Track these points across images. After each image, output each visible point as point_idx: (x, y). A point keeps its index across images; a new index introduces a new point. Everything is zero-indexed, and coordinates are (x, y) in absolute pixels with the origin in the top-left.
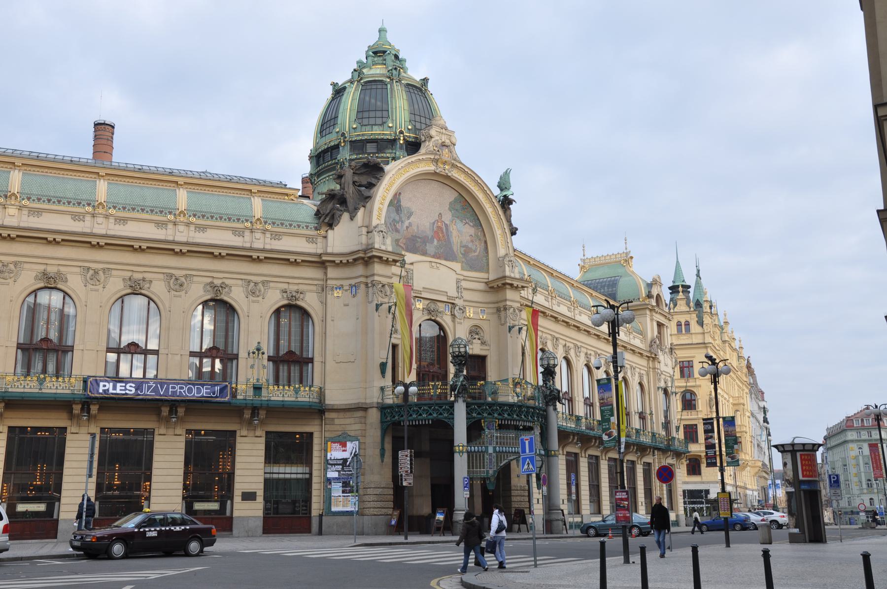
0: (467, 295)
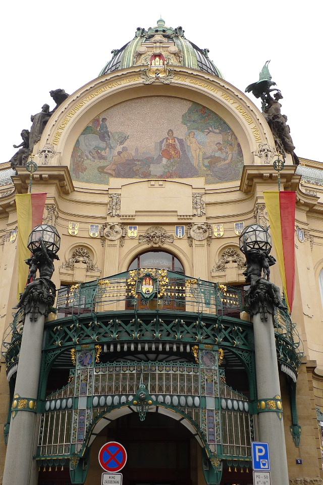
0: (213, 212)
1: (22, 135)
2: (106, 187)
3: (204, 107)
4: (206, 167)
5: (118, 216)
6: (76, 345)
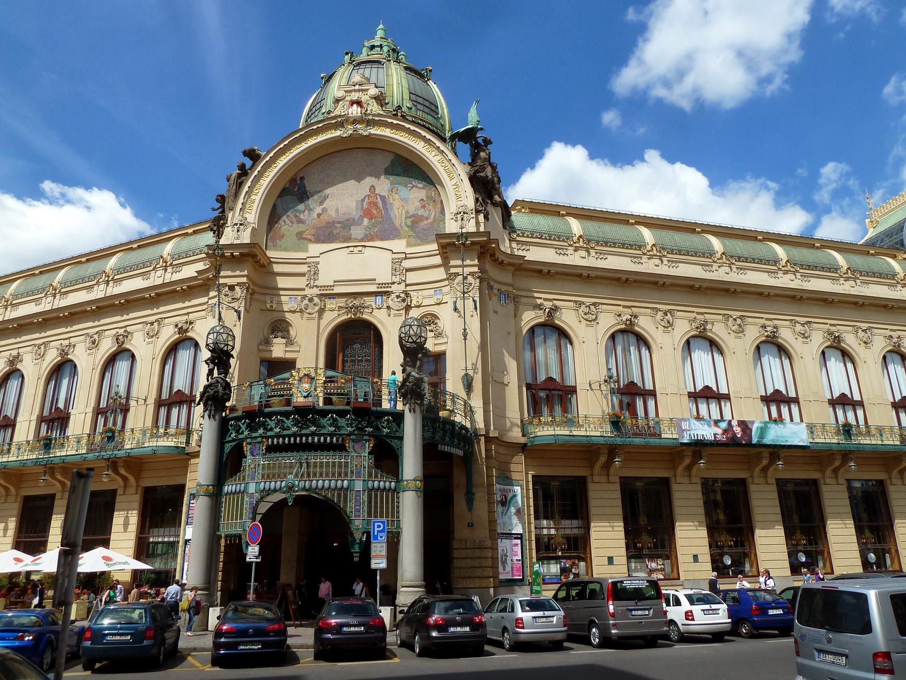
0: (412, 277)
1: (217, 200)
2: (303, 255)
3: (407, 159)
4: (408, 227)
5: (317, 287)
6: (246, 438)
